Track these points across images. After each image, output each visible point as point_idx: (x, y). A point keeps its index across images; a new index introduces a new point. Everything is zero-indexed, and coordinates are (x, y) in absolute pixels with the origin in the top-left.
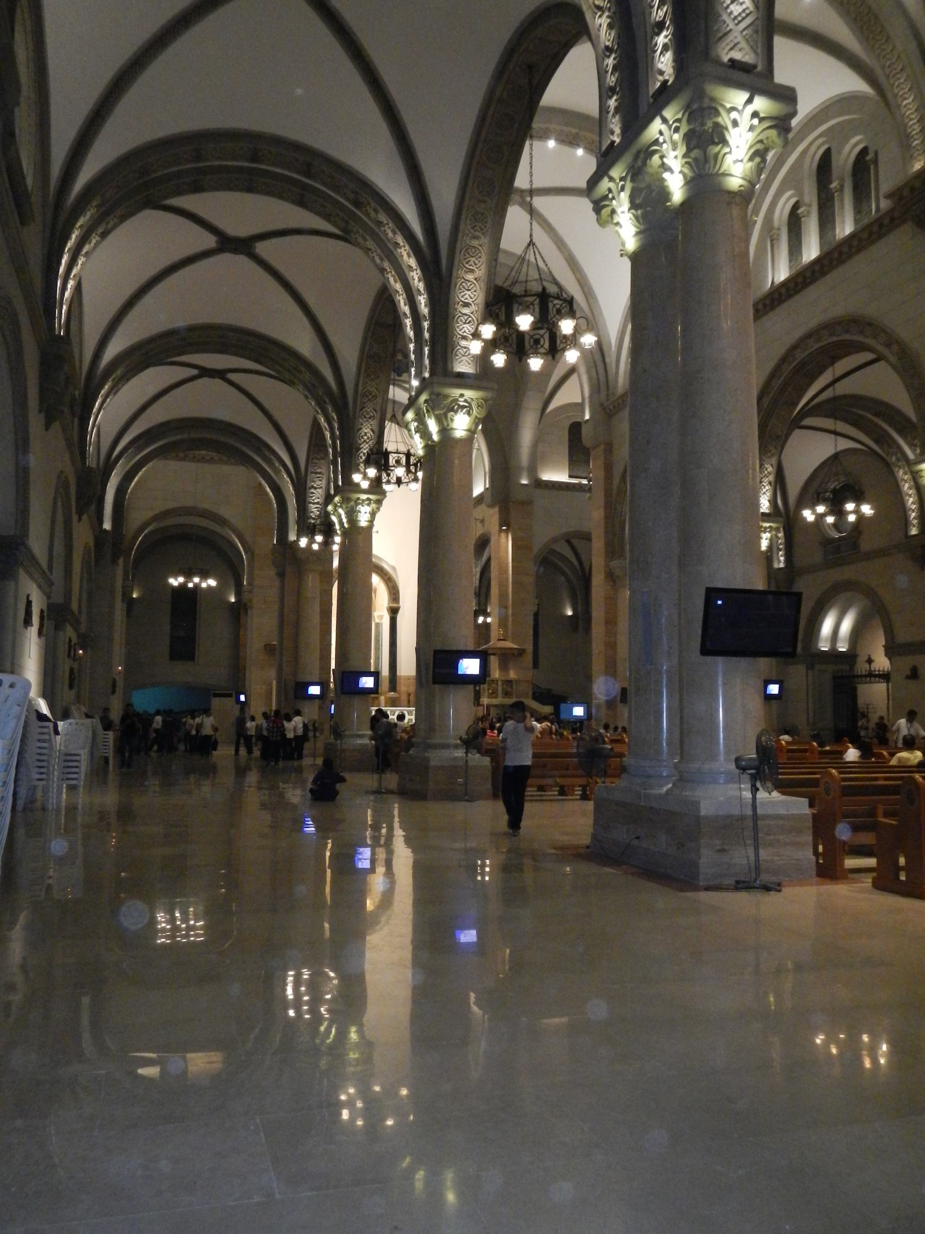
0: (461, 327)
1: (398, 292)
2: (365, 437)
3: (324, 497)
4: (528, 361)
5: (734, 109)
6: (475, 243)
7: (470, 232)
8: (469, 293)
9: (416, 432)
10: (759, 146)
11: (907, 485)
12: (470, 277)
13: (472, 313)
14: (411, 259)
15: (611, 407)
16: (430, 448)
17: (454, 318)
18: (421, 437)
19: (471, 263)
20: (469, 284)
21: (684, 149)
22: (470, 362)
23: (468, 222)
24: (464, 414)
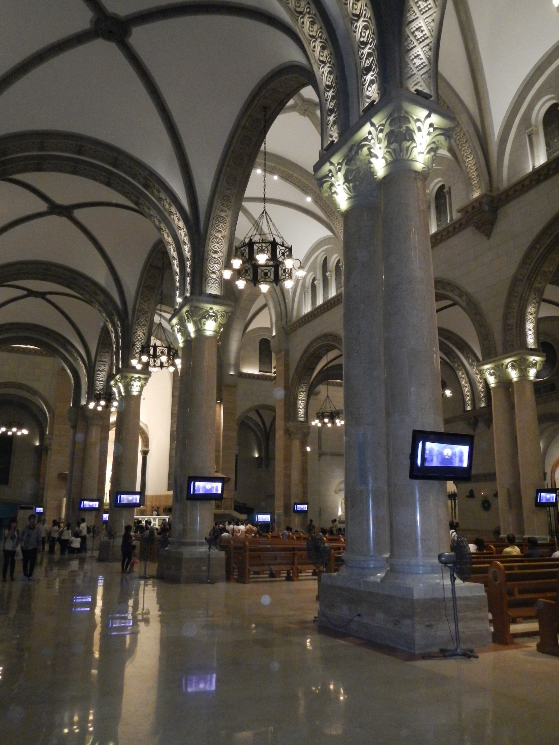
0: (212, 266)
1: (170, 243)
2: (139, 338)
3: (106, 376)
4: (260, 286)
5: (418, 120)
6: (223, 214)
7: (220, 207)
8: (218, 245)
9: (178, 332)
10: (433, 146)
11: (464, 381)
12: (219, 235)
13: (219, 257)
14: (180, 222)
15: (289, 329)
16: (188, 342)
17: (207, 260)
18: (182, 335)
19: (220, 226)
20: (218, 239)
21: (386, 143)
22: (217, 287)
23: (219, 201)
24: (212, 320)
